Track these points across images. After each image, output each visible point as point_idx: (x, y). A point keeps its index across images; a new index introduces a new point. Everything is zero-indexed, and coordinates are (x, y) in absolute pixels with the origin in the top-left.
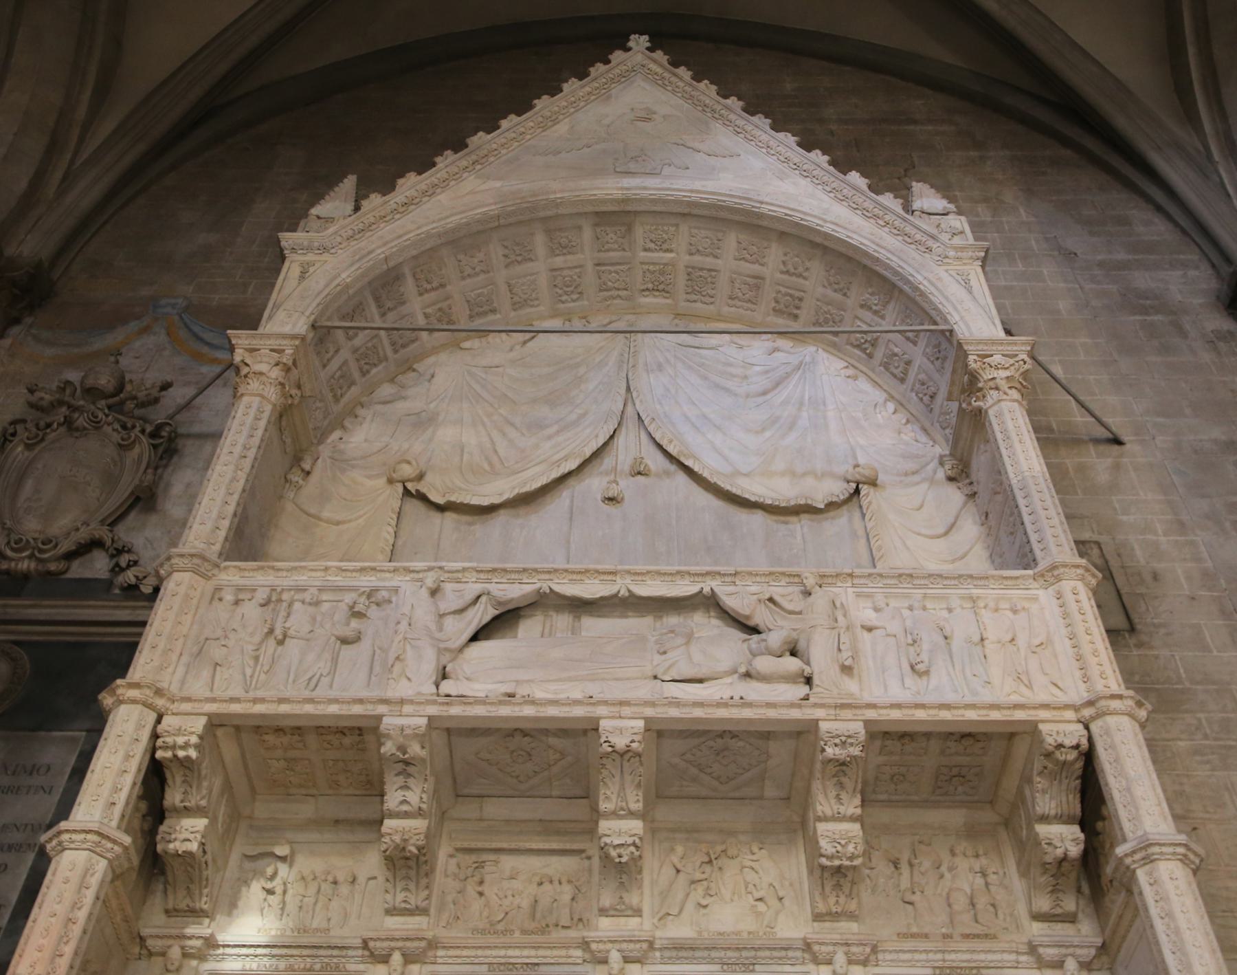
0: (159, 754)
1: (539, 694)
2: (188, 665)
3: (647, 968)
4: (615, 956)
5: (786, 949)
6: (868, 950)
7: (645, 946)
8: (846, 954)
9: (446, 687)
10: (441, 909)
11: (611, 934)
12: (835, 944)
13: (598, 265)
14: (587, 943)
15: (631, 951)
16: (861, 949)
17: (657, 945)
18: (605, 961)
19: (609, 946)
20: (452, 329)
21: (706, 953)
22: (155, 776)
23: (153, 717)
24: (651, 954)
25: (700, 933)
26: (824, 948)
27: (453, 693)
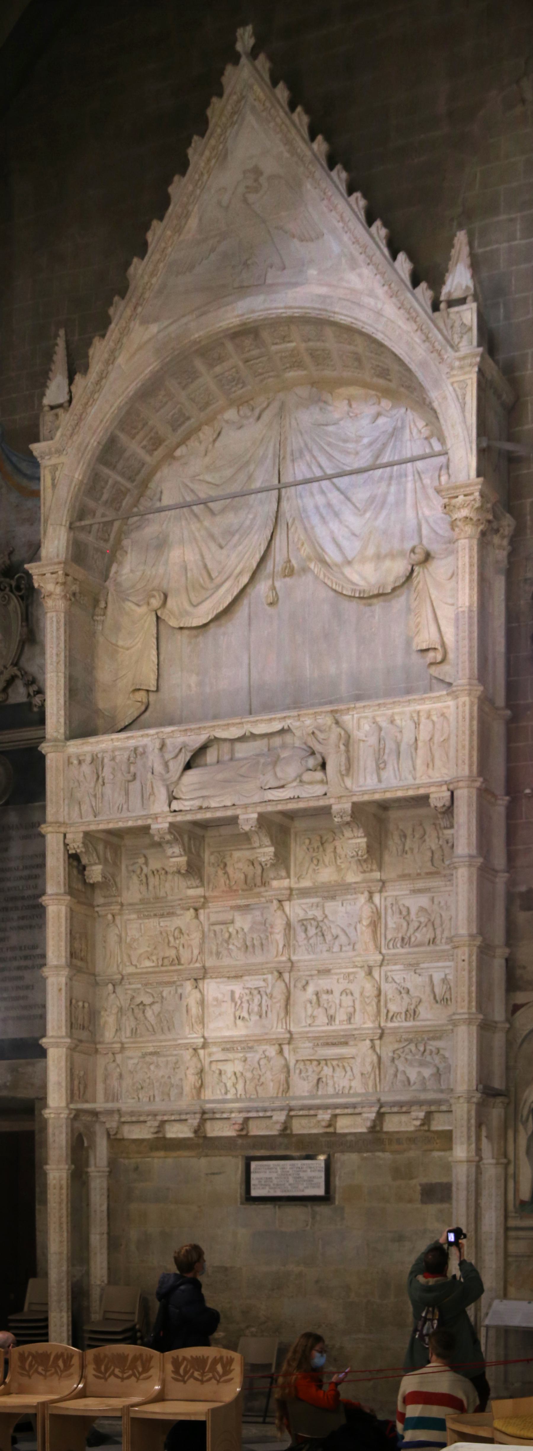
0: (70, 852)
1: (213, 804)
2: (69, 805)
9: (175, 805)
10: (209, 883)
13: (247, 361)
20: (164, 447)
22: (74, 859)
23: (62, 836)
27: (177, 809)
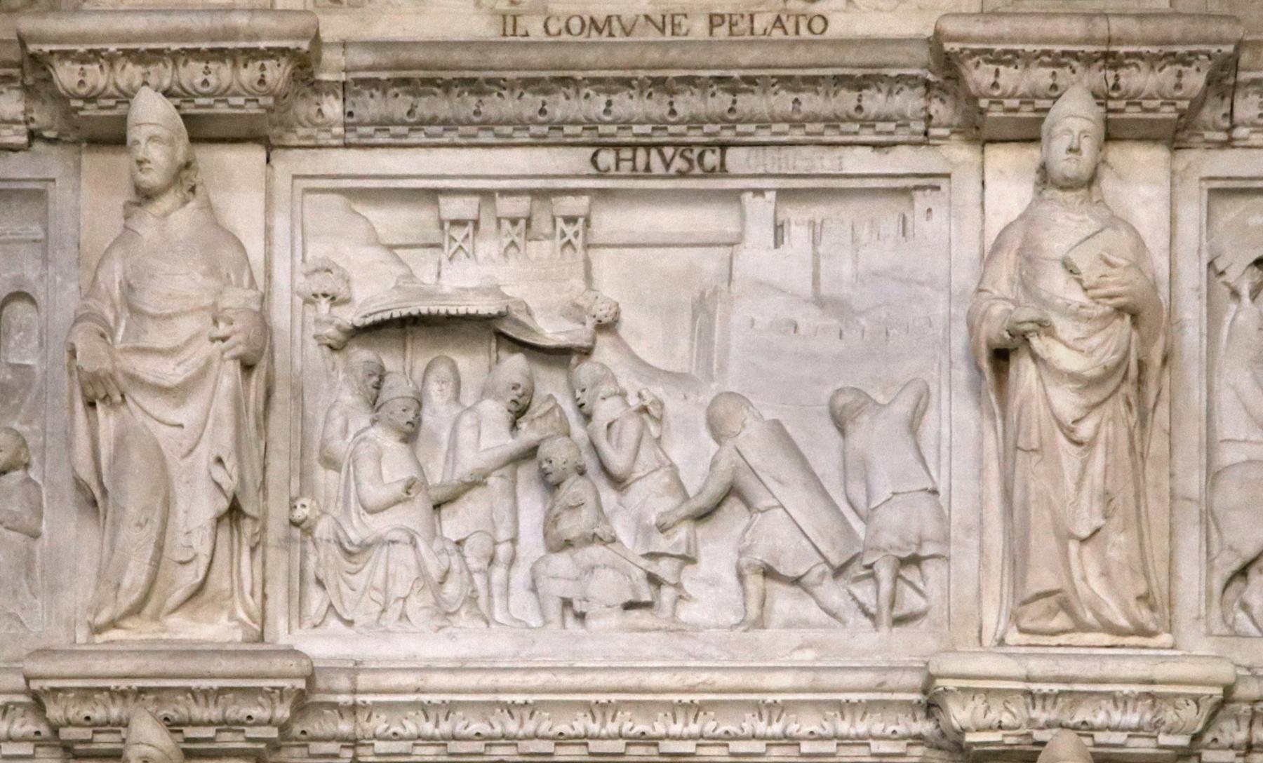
3: (289, 164)
4: (152, 114)
5: (859, 84)
6: (1195, 80)
7: (277, 73)
8: (1100, 98)
11: (138, 24)
12: (1058, 61)
14: (39, 63)
15: (221, 95)
16: (1166, 77)
17: (331, 68)
18: (112, 137)
19: (130, 74)
21: (529, 105)
24: (303, 109)
25: (510, 21)
26: (1010, 77)
